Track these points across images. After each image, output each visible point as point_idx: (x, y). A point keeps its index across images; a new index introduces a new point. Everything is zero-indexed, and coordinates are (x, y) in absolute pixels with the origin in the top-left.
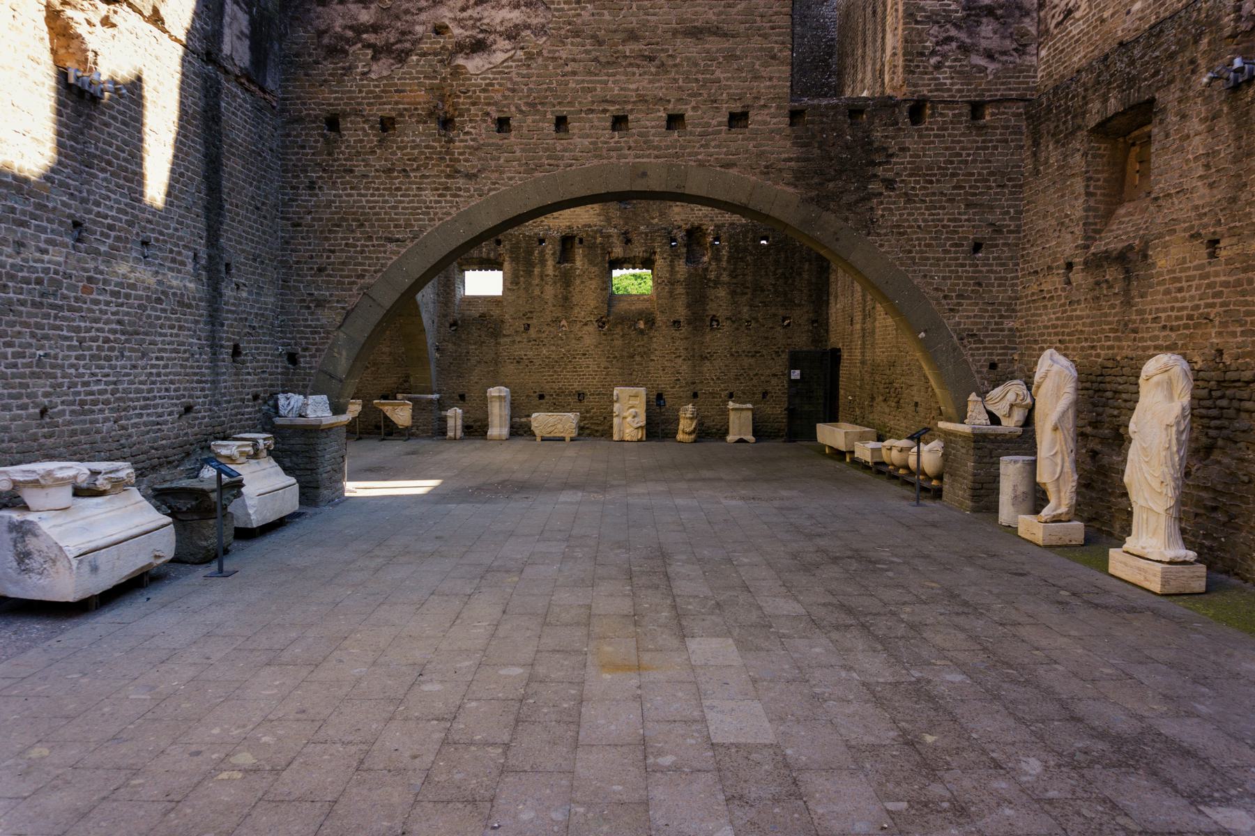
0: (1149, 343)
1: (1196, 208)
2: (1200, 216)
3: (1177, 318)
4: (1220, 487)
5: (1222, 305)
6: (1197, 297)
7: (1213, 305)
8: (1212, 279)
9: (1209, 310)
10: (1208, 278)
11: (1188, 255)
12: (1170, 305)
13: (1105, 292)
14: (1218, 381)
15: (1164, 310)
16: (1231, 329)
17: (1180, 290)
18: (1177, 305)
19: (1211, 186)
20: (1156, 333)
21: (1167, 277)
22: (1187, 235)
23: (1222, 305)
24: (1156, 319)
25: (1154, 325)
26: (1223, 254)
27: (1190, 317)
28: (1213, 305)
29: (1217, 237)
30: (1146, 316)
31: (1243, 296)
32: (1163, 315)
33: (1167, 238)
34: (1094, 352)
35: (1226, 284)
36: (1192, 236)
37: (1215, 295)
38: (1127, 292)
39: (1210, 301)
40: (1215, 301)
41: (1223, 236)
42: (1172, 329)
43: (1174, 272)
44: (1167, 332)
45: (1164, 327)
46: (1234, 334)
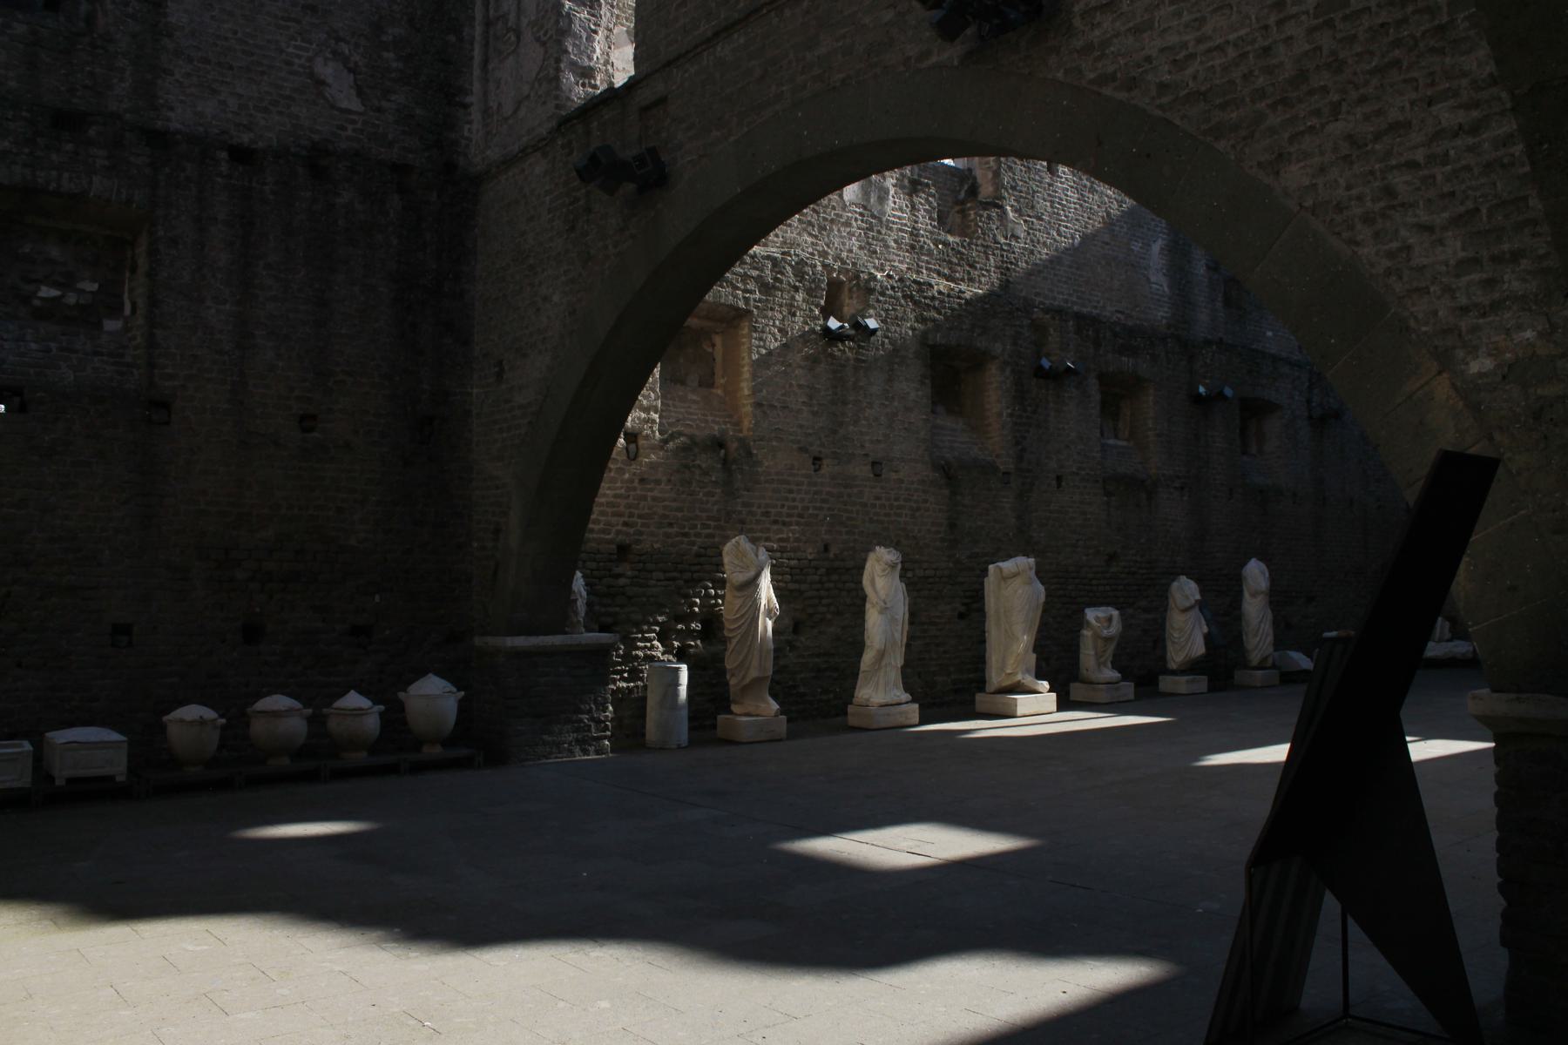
0: (758, 534)
1: (801, 426)
3: (789, 515)
5: (829, 509)
7: (821, 509)
12: (779, 503)
13: (698, 478)
17: (791, 491)
18: (787, 503)
19: (815, 414)
20: (768, 526)
22: (795, 446)
24: (767, 514)
25: (763, 518)
26: (825, 470)
27: (800, 516)
28: (821, 509)
30: (754, 509)
32: (773, 510)
33: (774, 443)
34: (686, 540)
37: (824, 501)
39: (818, 505)
42: (784, 524)
45: (775, 522)
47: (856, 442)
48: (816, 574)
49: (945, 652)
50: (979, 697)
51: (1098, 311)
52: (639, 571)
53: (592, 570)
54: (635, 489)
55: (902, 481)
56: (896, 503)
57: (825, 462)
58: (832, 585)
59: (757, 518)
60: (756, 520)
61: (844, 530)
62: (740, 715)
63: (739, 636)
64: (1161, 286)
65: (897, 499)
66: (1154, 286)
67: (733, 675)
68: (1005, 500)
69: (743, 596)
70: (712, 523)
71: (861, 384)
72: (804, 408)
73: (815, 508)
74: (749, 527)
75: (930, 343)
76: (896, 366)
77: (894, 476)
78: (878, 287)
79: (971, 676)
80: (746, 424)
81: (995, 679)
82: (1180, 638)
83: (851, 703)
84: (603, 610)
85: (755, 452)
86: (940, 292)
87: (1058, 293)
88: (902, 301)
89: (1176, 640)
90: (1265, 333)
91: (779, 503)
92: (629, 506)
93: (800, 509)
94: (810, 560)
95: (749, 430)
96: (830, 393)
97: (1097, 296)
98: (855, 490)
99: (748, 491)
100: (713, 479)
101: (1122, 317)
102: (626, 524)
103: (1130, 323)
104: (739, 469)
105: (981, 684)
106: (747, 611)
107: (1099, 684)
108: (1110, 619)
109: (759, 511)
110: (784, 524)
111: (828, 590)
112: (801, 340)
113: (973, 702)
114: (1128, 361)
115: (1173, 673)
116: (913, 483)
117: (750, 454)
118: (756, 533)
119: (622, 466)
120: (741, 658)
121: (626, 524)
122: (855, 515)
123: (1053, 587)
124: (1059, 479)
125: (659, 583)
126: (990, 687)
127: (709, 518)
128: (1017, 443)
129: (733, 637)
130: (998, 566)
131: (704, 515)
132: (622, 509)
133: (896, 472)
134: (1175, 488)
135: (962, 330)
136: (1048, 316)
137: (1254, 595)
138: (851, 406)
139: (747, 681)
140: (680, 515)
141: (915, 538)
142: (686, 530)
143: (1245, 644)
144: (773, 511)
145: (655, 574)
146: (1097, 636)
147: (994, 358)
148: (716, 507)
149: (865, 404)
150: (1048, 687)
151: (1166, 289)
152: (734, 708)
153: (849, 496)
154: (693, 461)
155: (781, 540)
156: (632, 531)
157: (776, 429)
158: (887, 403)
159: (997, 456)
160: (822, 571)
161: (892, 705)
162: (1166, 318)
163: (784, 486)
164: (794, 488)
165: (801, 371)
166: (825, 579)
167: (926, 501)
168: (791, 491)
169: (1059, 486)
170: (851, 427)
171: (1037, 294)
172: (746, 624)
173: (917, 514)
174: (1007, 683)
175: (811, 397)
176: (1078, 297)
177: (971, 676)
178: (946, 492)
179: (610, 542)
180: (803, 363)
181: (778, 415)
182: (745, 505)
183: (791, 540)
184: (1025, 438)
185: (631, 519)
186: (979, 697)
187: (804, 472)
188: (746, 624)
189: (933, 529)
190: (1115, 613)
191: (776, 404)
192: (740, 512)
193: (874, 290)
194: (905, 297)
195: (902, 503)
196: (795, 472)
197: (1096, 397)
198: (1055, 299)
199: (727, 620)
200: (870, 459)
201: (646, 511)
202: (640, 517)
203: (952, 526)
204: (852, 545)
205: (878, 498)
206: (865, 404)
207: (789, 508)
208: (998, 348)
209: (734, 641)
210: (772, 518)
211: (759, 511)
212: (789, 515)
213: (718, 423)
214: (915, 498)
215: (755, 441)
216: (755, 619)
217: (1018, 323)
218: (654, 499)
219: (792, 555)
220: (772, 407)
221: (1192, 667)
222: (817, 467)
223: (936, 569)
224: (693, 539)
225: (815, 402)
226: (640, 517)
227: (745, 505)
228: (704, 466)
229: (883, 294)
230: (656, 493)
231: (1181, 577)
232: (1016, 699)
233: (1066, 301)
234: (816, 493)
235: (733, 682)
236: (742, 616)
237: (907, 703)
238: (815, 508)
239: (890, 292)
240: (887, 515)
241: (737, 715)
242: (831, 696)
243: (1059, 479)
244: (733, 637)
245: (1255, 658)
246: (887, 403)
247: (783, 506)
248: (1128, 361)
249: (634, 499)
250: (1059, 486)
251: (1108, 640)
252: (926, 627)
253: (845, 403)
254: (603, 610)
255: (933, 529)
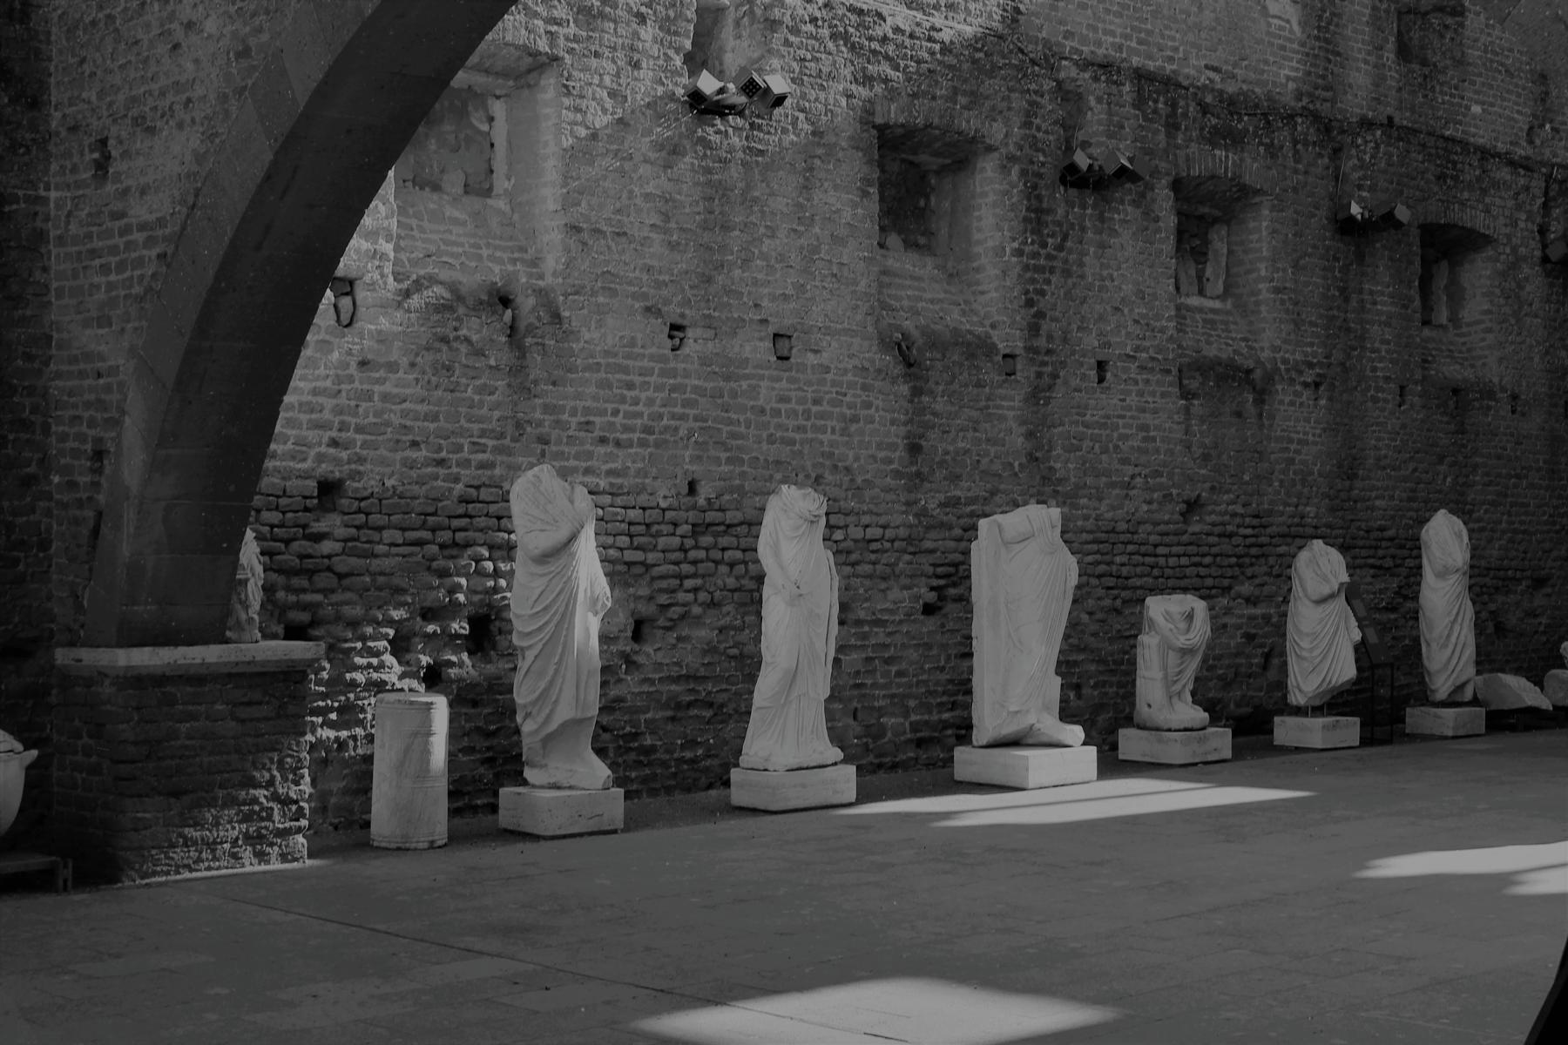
0: (572, 463)
1: (649, 269)
2: (659, 285)
3: (627, 429)
4: (702, 672)
5: (696, 419)
6: (658, 402)
7: (683, 417)
8: (679, 380)
9: (678, 423)
10: (675, 377)
11: (639, 336)
12: (610, 407)
13: (464, 361)
14: (694, 525)
15: (603, 413)
16: (712, 453)
17: (630, 386)
19: (673, 246)
20: (588, 447)
21: (602, 361)
23: (696, 419)
24: (587, 426)
25: (582, 434)
26: (690, 348)
27: (648, 430)
28: (683, 417)
29: (685, 323)
30: (565, 417)
31: (727, 411)
32: (597, 420)
33: (601, 299)
34: (442, 471)
35: (696, 389)
36: (648, 309)
37: (687, 403)
38: (518, 370)
39: (678, 410)
40: (687, 411)
41: (694, 325)
43: (615, 355)
44: (610, 448)
45: (603, 441)
46: (718, 461)
47: (745, 299)
48: (673, 534)
49: (900, 674)
50: (961, 753)
51: (1174, 67)
52: (358, 528)
53: (272, 526)
54: (351, 379)
55: (827, 370)
56: (815, 409)
57: (690, 333)
58: (702, 554)
59: (571, 433)
60: (569, 437)
61: (724, 455)
62: (542, 787)
63: (540, 646)
64: (1288, 21)
65: (816, 402)
66: (1276, 21)
67: (528, 715)
68: (1005, 403)
69: (544, 575)
70: (491, 443)
71: (756, 194)
72: (653, 235)
73: (673, 417)
74: (554, 448)
75: (879, 120)
76: (817, 162)
77: (811, 359)
78: (787, 19)
79: (946, 716)
80: (552, 262)
81: (988, 720)
82: (1311, 650)
83: (737, 765)
84: (292, 598)
85: (567, 314)
86: (897, 30)
87: (1106, 32)
88: (831, 45)
89: (1305, 654)
90: (1468, 108)
91: (610, 407)
92: (338, 411)
93: (646, 417)
94: (664, 510)
95: (555, 274)
96: (701, 208)
97: (1173, 39)
98: (745, 384)
99: (554, 384)
100: (492, 362)
101: (1217, 77)
102: (334, 443)
103: (1231, 88)
104: (537, 344)
105: (964, 731)
106: (554, 600)
107: (1169, 730)
108: (1190, 617)
109: (574, 420)
110: (618, 444)
111: (695, 563)
112: (649, 112)
113: (950, 760)
114: (1227, 157)
115: (1298, 711)
116: (846, 371)
117: (556, 317)
118: (568, 459)
119: (328, 338)
120: (543, 685)
121: (334, 443)
122: (742, 429)
123: (1090, 559)
124: (1101, 366)
125: (394, 550)
126: (981, 735)
127: (483, 433)
128: (1030, 303)
129: (530, 647)
130: (995, 521)
131: (475, 427)
132: (327, 415)
133: (816, 352)
134: (1306, 385)
135: (934, 98)
136: (1087, 75)
137: (1442, 575)
138: (737, 233)
139: (553, 726)
140: (432, 426)
141: (847, 469)
142: (443, 454)
143: (1426, 662)
144: (597, 420)
145: (387, 535)
146: (1166, 646)
147: (990, 149)
148: (497, 414)
149: (762, 230)
150: (1082, 735)
151: (1296, 28)
152: (528, 773)
153: (734, 394)
154: (456, 329)
155: (610, 473)
156: (344, 455)
157: (604, 273)
158: (802, 228)
159: (993, 326)
160: (685, 529)
161: (807, 768)
162: (1294, 79)
163: (618, 376)
164: (637, 379)
165: (648, 167)
166: (689, 542)
167: (868, 405)
168: (630, 386)
169: (1101, 380)
170: (737, 272)
171: (1068, 35)
172: (552, 625)
173: (853, 427)
174: (1009, 729)
175: (667, 217)
176: (1140, 42)
177: (946, 716)
178: (904, 389)
179: (305, 476)
180: (652, 155)
181: (609, 248)
182: (547, 409)
183: (632, 472)
184: (1042, 293)
185: (344, 435)
186: (961, 753)
187: (653, 350)
188: (552, 625)
189: (881, 454)
190: (1200, 606)
191: (605, 228)
192: (540, 424)
193: (781, 23)
194: (833, 36)
195: (825, 407)
196: (637, 350)
197: (1169, 221)
198: (1099, 44)
199: (518, 616)
200: (771, 330)
201: (372, 419)
202: (360, 429)
203: (914, 449)
204: (737, 482)
205: (783, 399)
206: (762, 230)
207: (627, 415)
208: (996, 132)
209: (530, 655)
210: (597, 433)
211: (574, 420)
212: (627, 429)
213: (500, 261)
214: (848, 399)
215: (566, 295)
216: (567, 616)
217: (1033, 86)
218: (385, 397)
219: (631, 500)
220: (597, 231)
221: (1335, 703)
222: (677, 341)
223: (884, 527)
224: (455, 470)
225: (673, 225)
226: (360, 429)
227: (547, 409)
228: (475, 338)
229: (795, 31)
230: (388, 387)
231: (1315, 541)
232: (1027, 758)
233: (1120, 48)
234: (673, 389)
235: (527, 728)
236: (545, 609)
237: (835, 764)
238: (673, 417)
239: (809, 28)
240: (799, 429)
241: (534, 786)
242: (700, 752)
243: (1101, 366)
244: (530, 647)
245: (1442, 687)
246: (802, 228)
247: (616, 413)
248: (1227, 157)
249: (564, 407)
250: (1101, 380)
251: (1186, 652)
252: (866, 629)
253: (726, 228)
254: (292, 598)
255: (881, 454)
